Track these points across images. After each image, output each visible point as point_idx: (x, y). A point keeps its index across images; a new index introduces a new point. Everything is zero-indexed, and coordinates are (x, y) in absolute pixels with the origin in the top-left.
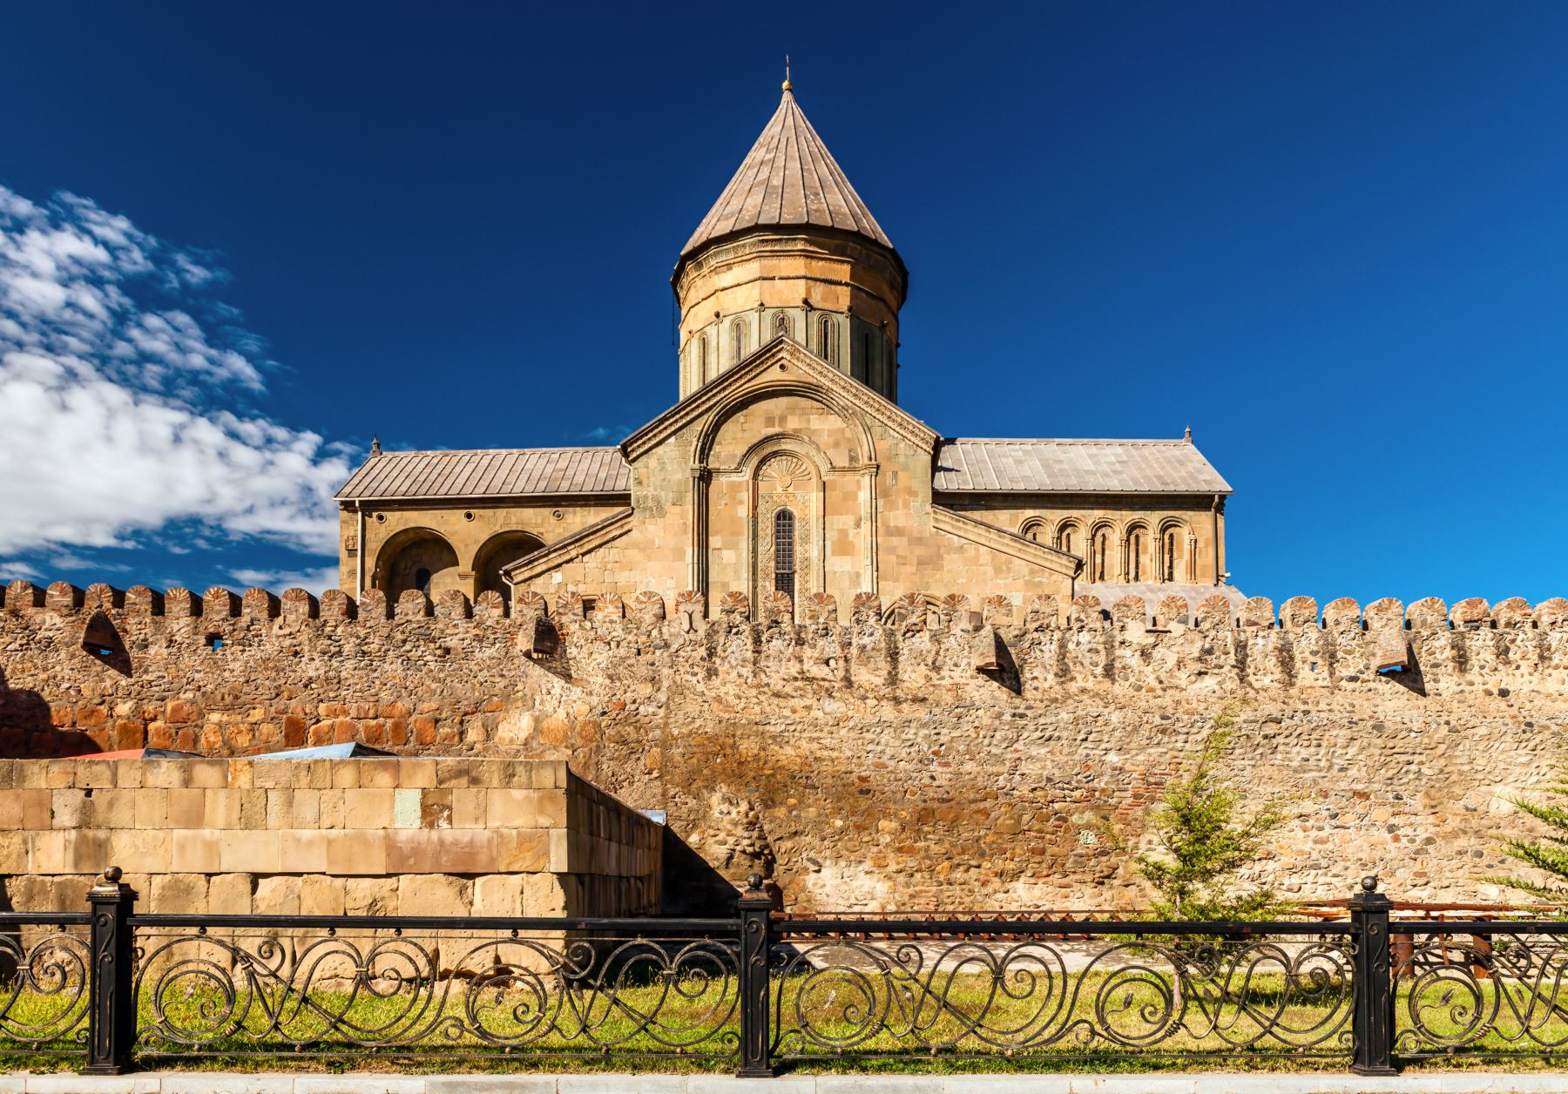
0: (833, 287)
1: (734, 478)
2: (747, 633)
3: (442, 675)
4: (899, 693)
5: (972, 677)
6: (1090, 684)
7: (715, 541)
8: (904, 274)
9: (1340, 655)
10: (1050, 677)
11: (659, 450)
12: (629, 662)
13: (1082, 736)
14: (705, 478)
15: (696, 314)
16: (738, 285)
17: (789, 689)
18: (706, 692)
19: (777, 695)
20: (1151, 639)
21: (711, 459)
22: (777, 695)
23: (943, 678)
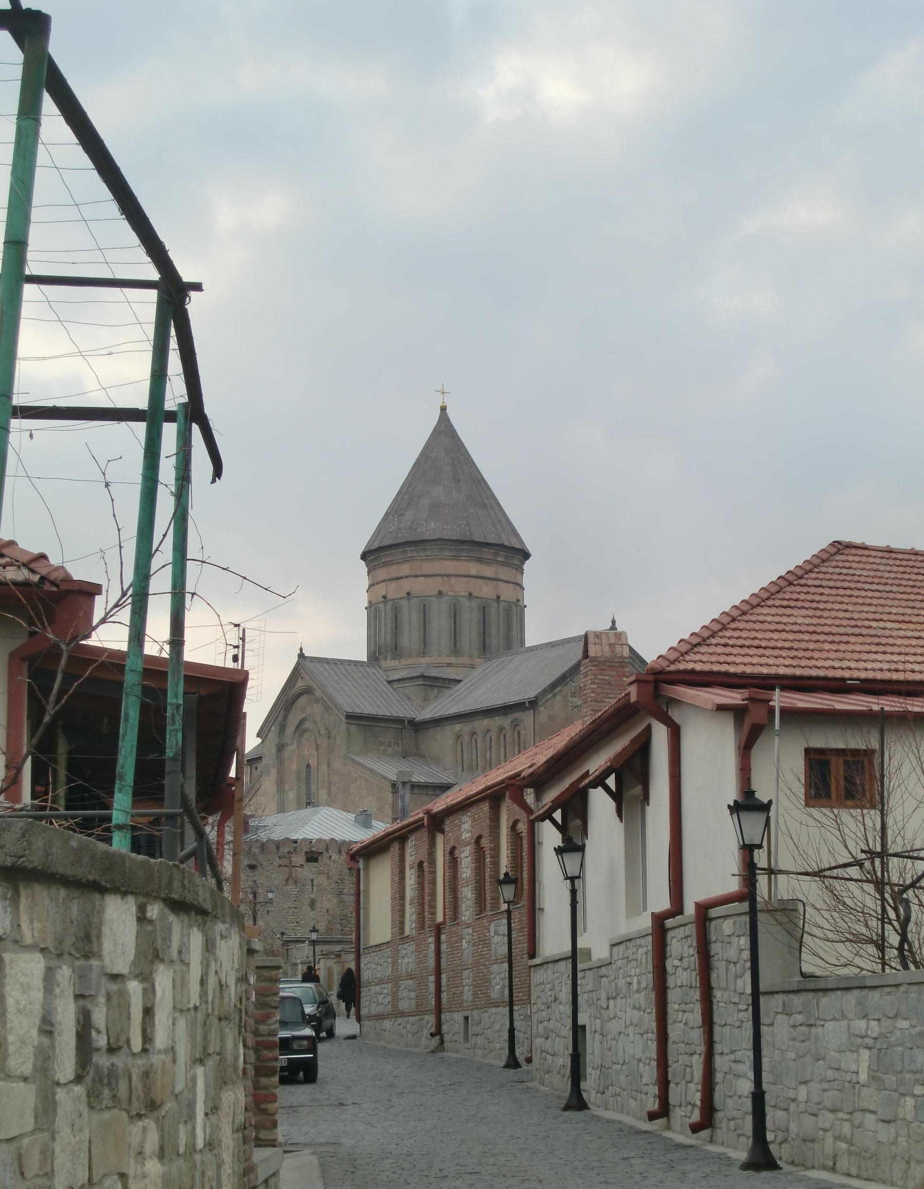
0: (400, 581)
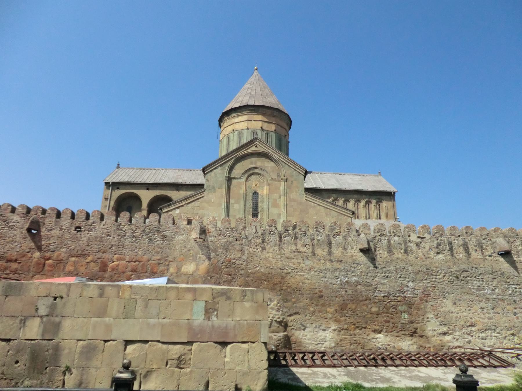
1: (239, 181)
2: (276, 234)
3: (162, 246)
4: (332, 258)
5: (358, 253)
6: (400, 256)
7: (232, 201)
8: (291, 122)
9: (484, 247)
10: (386, 253)
11: (215, 171)
12: (233, 244)
13: (399, 276)
14: (229, 180)
15: (226, 130)
16: (241, 122)
17: (292, 256)
18: (261, 256)
19: (288, 258)
20: (419, 240)
21: (232, 174)
22: (288, 258)
23: (348, 253)
